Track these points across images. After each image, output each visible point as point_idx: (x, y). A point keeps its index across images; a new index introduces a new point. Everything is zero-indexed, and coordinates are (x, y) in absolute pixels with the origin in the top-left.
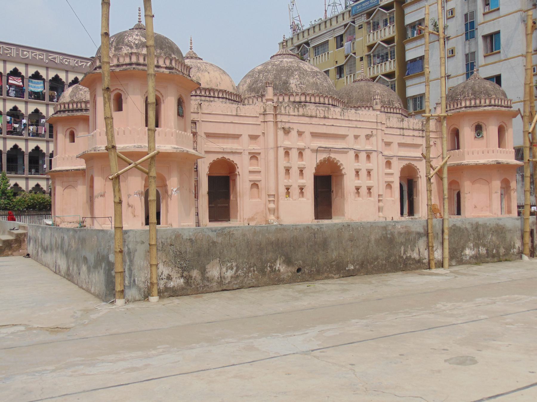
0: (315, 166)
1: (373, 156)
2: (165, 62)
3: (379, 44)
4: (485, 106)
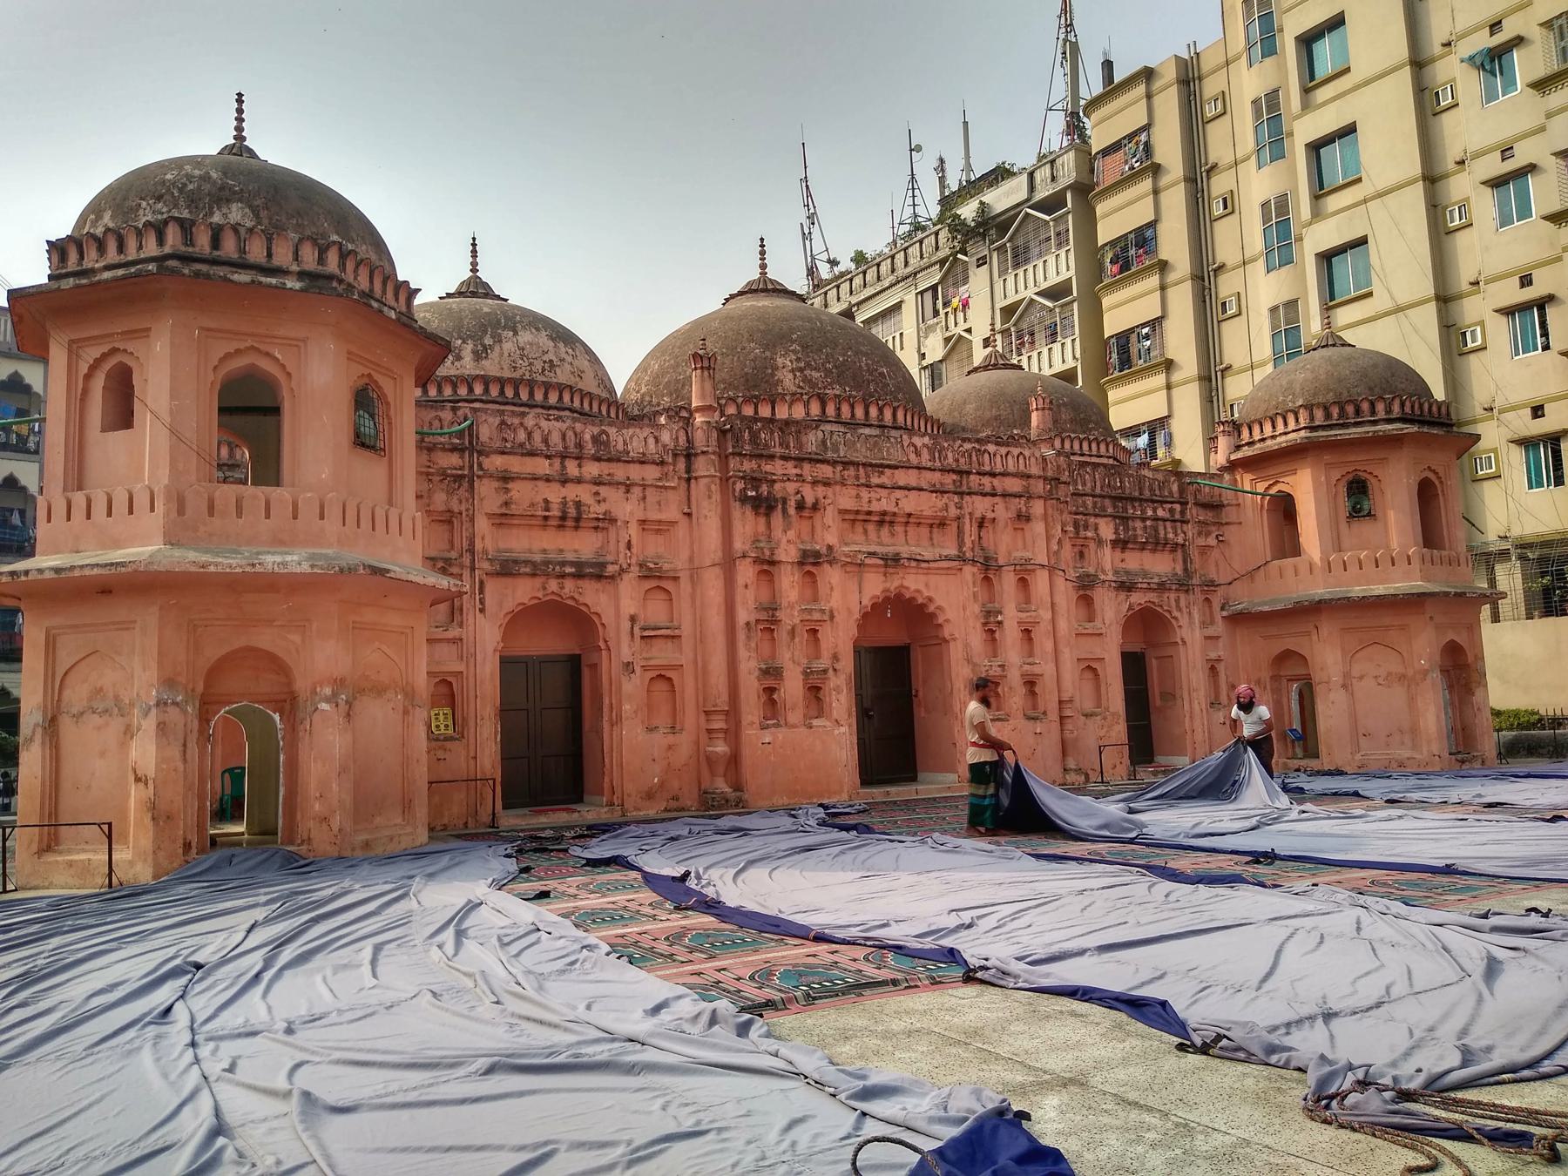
0: (857, 616)
1: (1040, 582)
2: (296, 258)
3: (1032, 300)
4: (1374, 423)
